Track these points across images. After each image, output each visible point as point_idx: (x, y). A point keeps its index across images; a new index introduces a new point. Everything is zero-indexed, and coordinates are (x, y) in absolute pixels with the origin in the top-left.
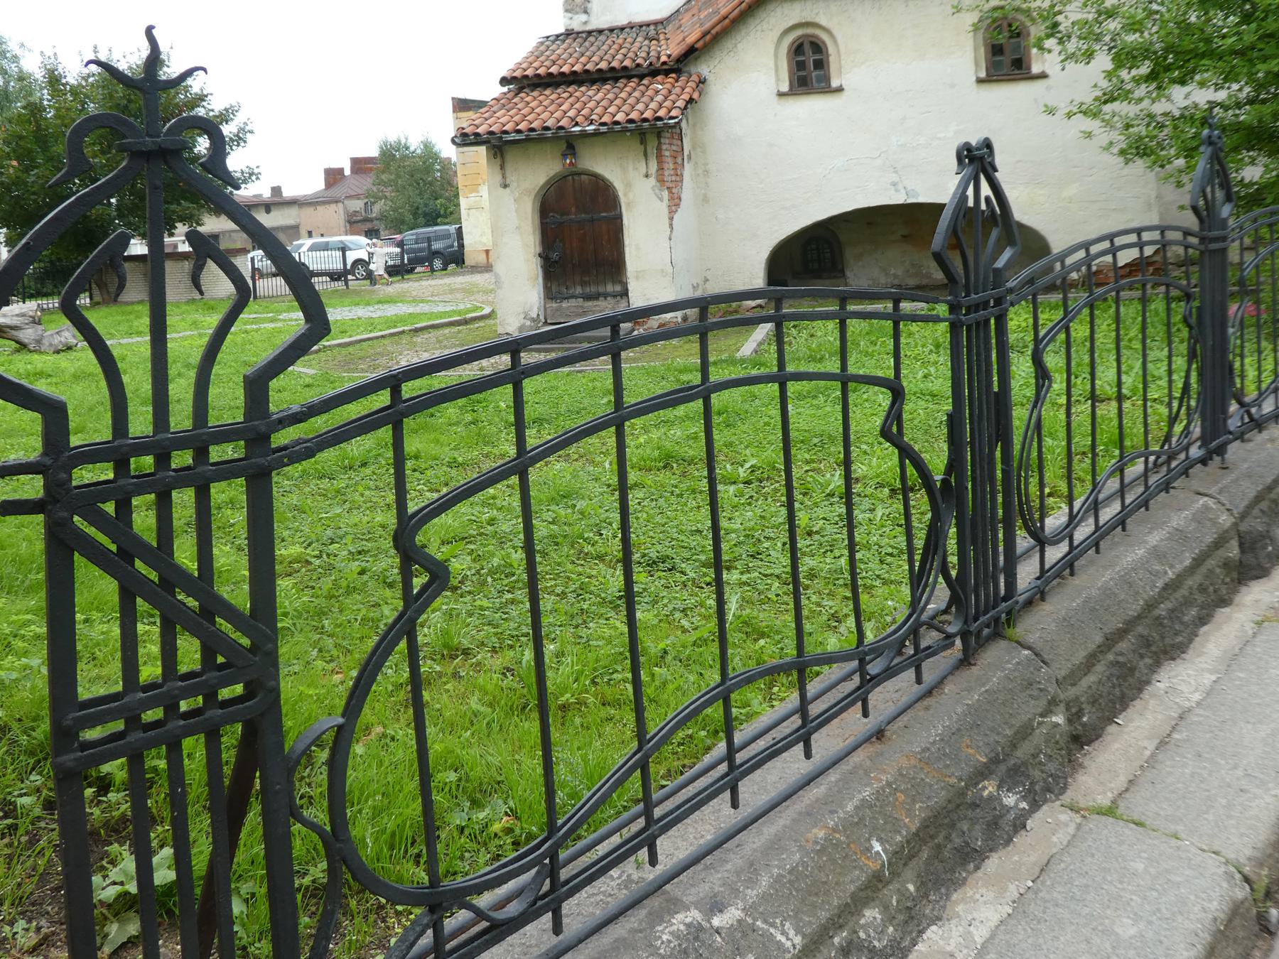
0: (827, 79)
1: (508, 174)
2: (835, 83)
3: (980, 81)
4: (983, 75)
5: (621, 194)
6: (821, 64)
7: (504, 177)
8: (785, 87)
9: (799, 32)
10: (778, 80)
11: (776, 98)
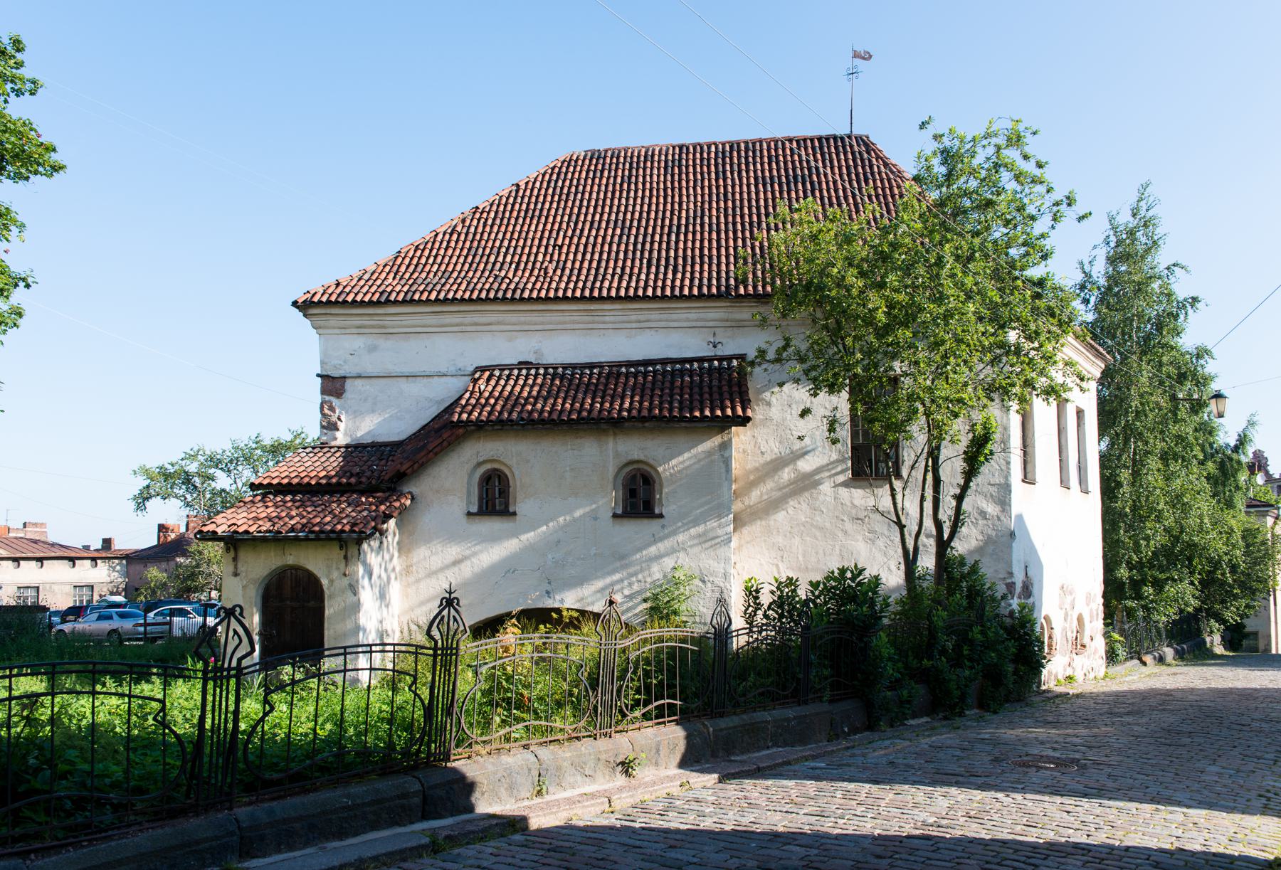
0: (507, 505)
1: (239, 565)
2: (511, 510)
3: (615, 516)
4: (620, 511)
5: (325, 588)
6: (505, 492)
7: (236, 567)
8: (474, 509)
9: (489, 466)
10: (469, 503)
11: (464, 519)
